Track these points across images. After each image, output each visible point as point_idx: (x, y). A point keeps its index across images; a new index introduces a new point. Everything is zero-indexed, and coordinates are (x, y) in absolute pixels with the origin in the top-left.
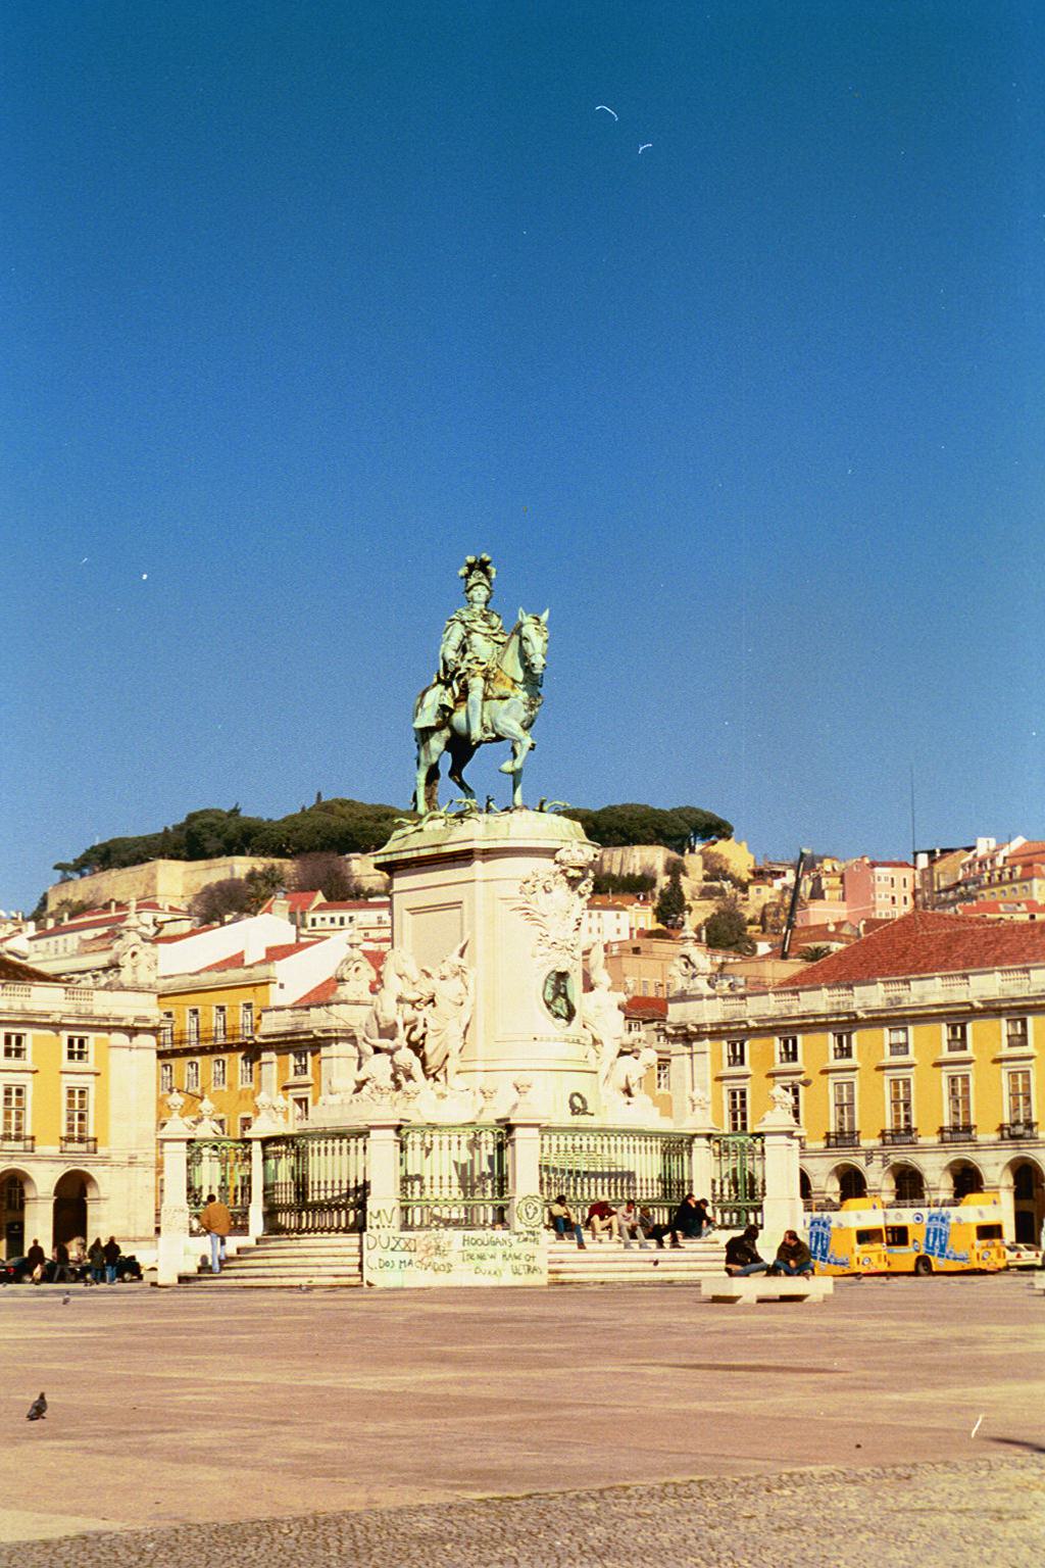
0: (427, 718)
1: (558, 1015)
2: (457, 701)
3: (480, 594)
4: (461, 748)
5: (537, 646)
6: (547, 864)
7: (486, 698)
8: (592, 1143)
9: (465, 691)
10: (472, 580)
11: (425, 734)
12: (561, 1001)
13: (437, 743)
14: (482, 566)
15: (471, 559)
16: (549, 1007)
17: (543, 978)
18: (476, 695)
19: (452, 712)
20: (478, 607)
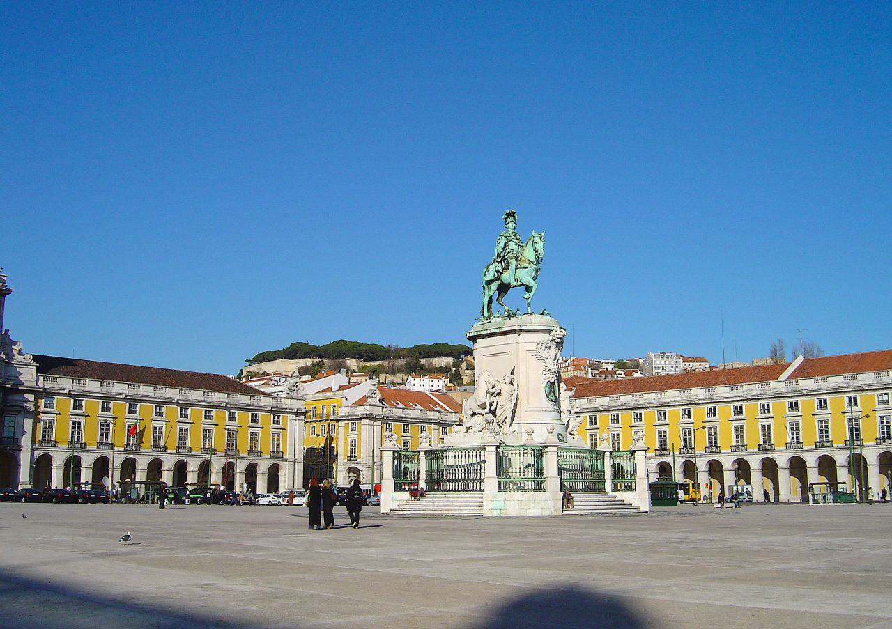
0: (490, 277)
1: (551, 400)
2: (503, 270)
3: (511, 226)
4: (504, 288)
5: (540, 246)
6: (546, 337)
7: (517, 268)
8: (565, 454)
9: (508, 265)
10: (509, 220)
11: (489, 282)
12: (552, 394)
13: (494, 287)
14: (512, 214)
15: (508, 212)
16: (548, 397)
17: (545, 384)
18: (512, 267)
19: (501, 273)
20: (511, 231)
